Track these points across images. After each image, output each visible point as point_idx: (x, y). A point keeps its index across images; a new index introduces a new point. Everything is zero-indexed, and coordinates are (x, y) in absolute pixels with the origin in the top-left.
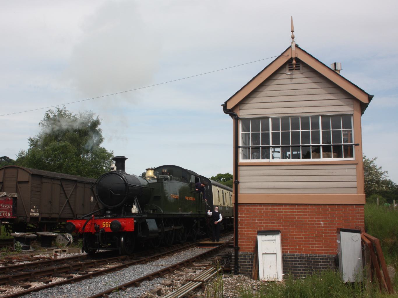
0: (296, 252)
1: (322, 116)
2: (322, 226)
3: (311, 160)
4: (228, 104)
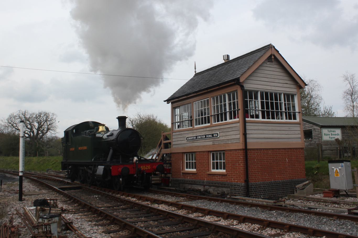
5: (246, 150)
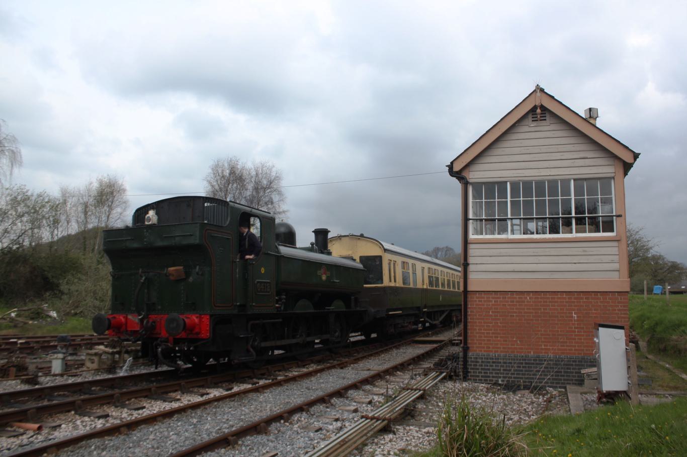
0: (542, 353)
1: (575, 180)
2: (574, 320)
3: (560, 236)
4: (454, 165)
5: (466, 292)
